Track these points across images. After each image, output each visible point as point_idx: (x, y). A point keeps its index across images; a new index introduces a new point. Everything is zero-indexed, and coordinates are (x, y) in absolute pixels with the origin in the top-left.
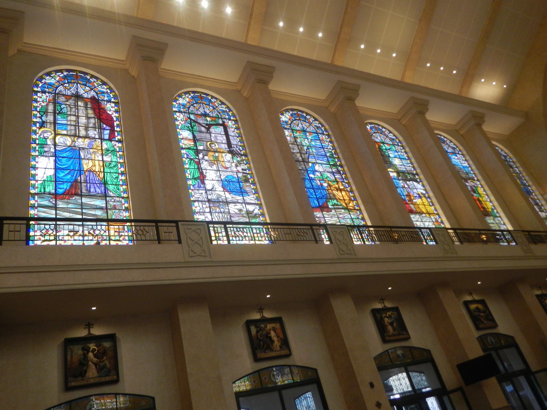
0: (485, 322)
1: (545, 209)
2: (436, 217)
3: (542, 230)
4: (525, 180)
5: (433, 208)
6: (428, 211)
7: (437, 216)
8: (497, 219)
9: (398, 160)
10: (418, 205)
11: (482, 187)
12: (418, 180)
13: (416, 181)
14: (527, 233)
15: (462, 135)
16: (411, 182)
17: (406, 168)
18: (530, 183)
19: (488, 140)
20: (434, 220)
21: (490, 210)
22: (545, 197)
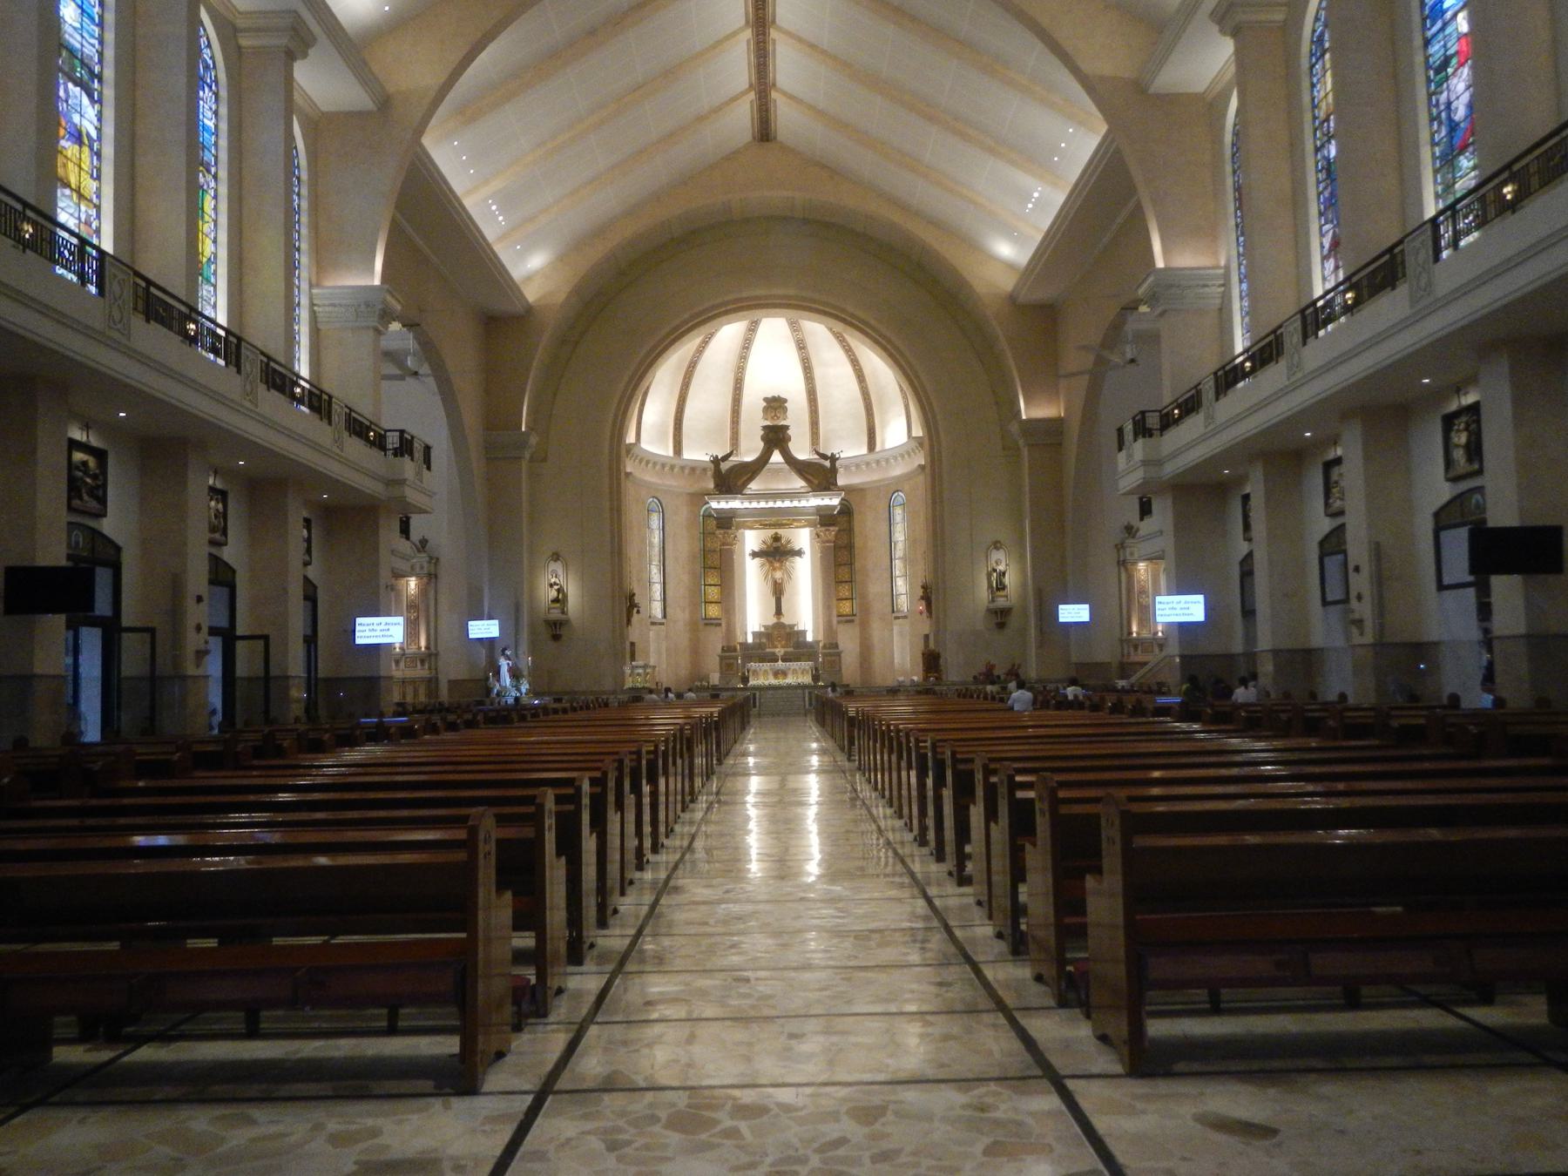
0: (86, 497)
1: (299, 316)
2: (90, 212)
3: (283, 361)
4: (299, 232)
5: (95, 184)
6: (79, 188)
7: (93, 212)
8: (206, 287)
9: (75, 10)
10: (66, 157)
11: (215, 197)
12: (96, 93)
13: (90, 95)
14: (265, 360)
15: (239, 47)
16: (78, 89)
17: (82, 45)
18: (304, 246)
19: (289, 108)
20: (83, 217)
21: (205, 260)
22: (315, 291)
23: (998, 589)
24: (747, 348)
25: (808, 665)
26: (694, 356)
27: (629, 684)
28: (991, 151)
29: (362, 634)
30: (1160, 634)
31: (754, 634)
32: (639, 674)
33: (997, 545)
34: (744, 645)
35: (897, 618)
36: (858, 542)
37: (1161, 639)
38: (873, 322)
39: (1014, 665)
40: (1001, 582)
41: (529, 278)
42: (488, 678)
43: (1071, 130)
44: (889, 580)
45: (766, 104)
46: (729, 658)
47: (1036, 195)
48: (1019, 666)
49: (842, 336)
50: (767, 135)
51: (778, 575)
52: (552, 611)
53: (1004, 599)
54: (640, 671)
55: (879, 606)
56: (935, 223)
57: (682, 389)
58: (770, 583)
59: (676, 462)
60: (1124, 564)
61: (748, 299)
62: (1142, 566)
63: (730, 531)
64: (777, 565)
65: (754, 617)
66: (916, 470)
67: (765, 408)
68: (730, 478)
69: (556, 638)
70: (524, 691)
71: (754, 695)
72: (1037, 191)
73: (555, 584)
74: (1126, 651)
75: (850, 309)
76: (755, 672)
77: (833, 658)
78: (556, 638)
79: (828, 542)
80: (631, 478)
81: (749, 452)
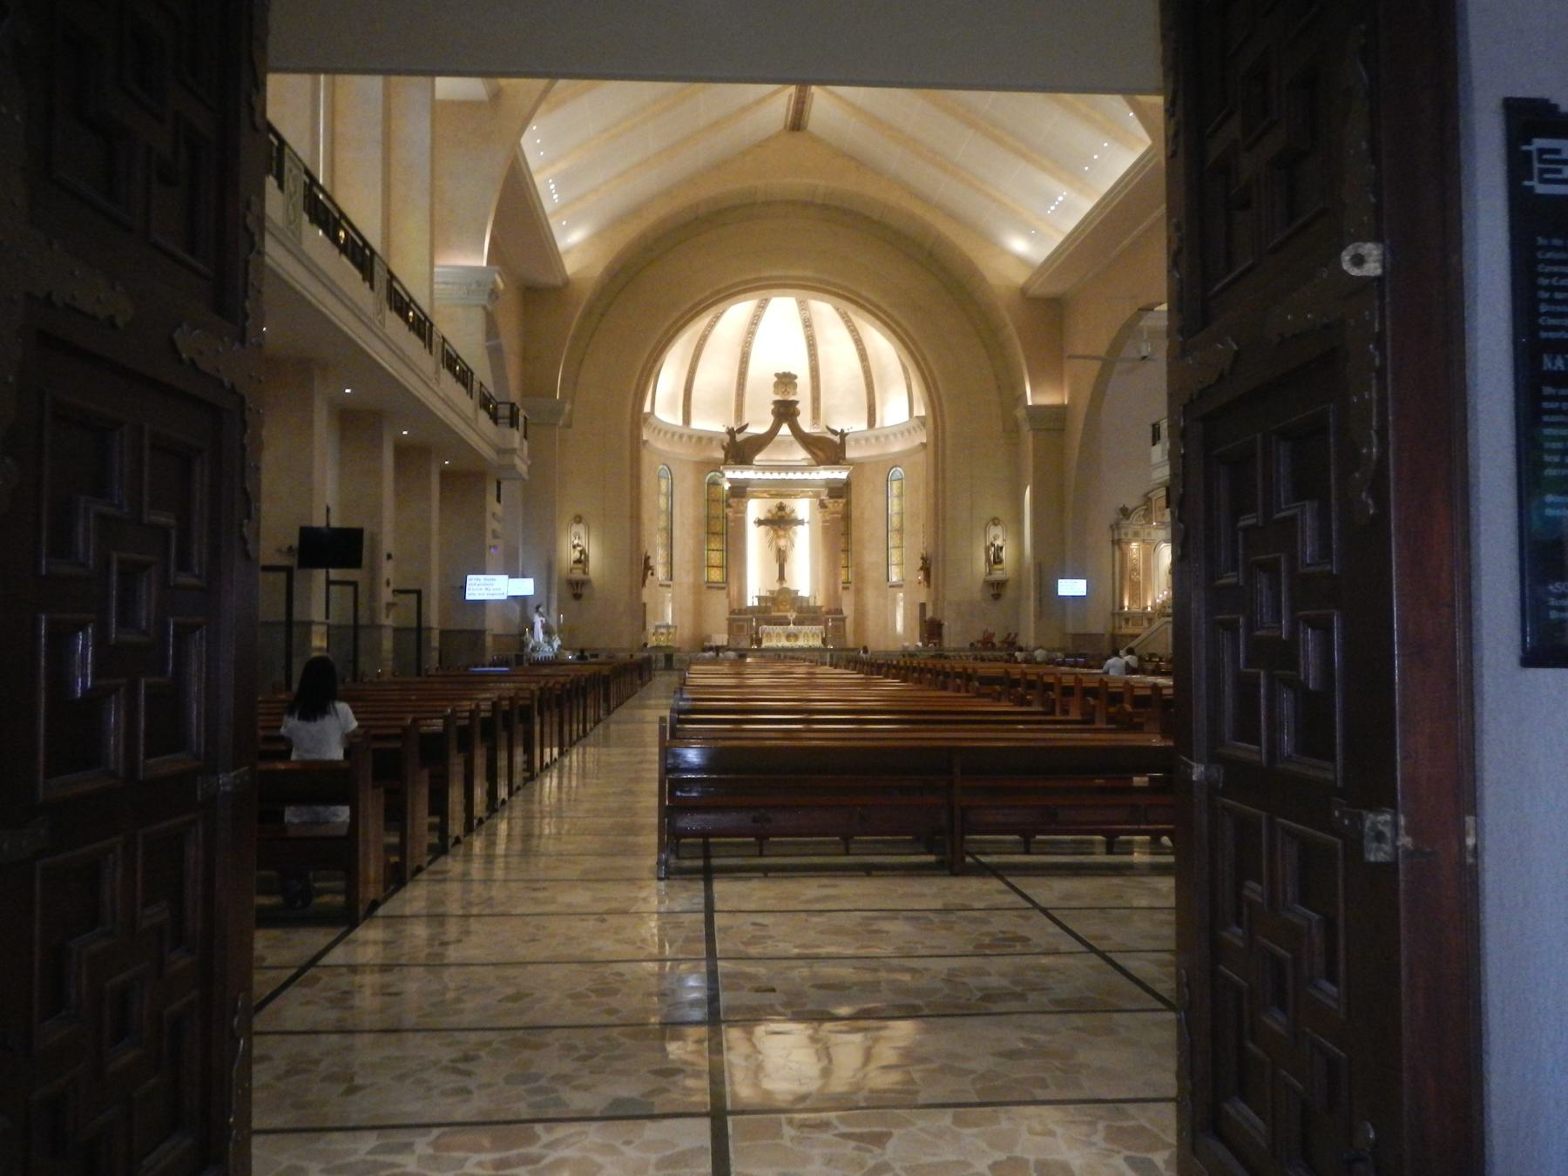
23: (995, 563)
24: (756, 324)
25: (818, 629)
26: (706, 330)
28: (1024, 156)
29: (472, 587)
30: (1149, 609)
31: (760, 598)
32: (662, 634)
33: (995, 521)
35: (891, 587)
36: (855, 513)
37: (1149, 613)
38: (885, 306)
39: (1009, 635)
40: (998, 557)
41: (568, 251)
42: (523, 634)
43: (1106, 145)
45: (804, 97)
46: (735, 620)
47: (1060, 199)
48: (1016, 635)
49: (846, 313)
50: (799, 125)
51: (782, 543)
53: (1000, 572)
54: (664, 630)
55: (873, 575)
56: (952, 216)
58: (774, 550)
59: (686, 431)
60: (1117, 543)
61: (767, 279)
62: (1134, 545)
63: (744, 500)
64: (781, 533)
65: (756, 583)
66: (918, 446)
67: (775, 383)
68: (741, 449)
69: (577, 597)
70: (556, 646)
72: (1062, 195)
73: (578, 545)
74: (1117, 621)
75: (864, 293)
76: (769, 635)
77: (838, 623)
78: (577, 597)
79: (837, 513)
81: (759, 425)
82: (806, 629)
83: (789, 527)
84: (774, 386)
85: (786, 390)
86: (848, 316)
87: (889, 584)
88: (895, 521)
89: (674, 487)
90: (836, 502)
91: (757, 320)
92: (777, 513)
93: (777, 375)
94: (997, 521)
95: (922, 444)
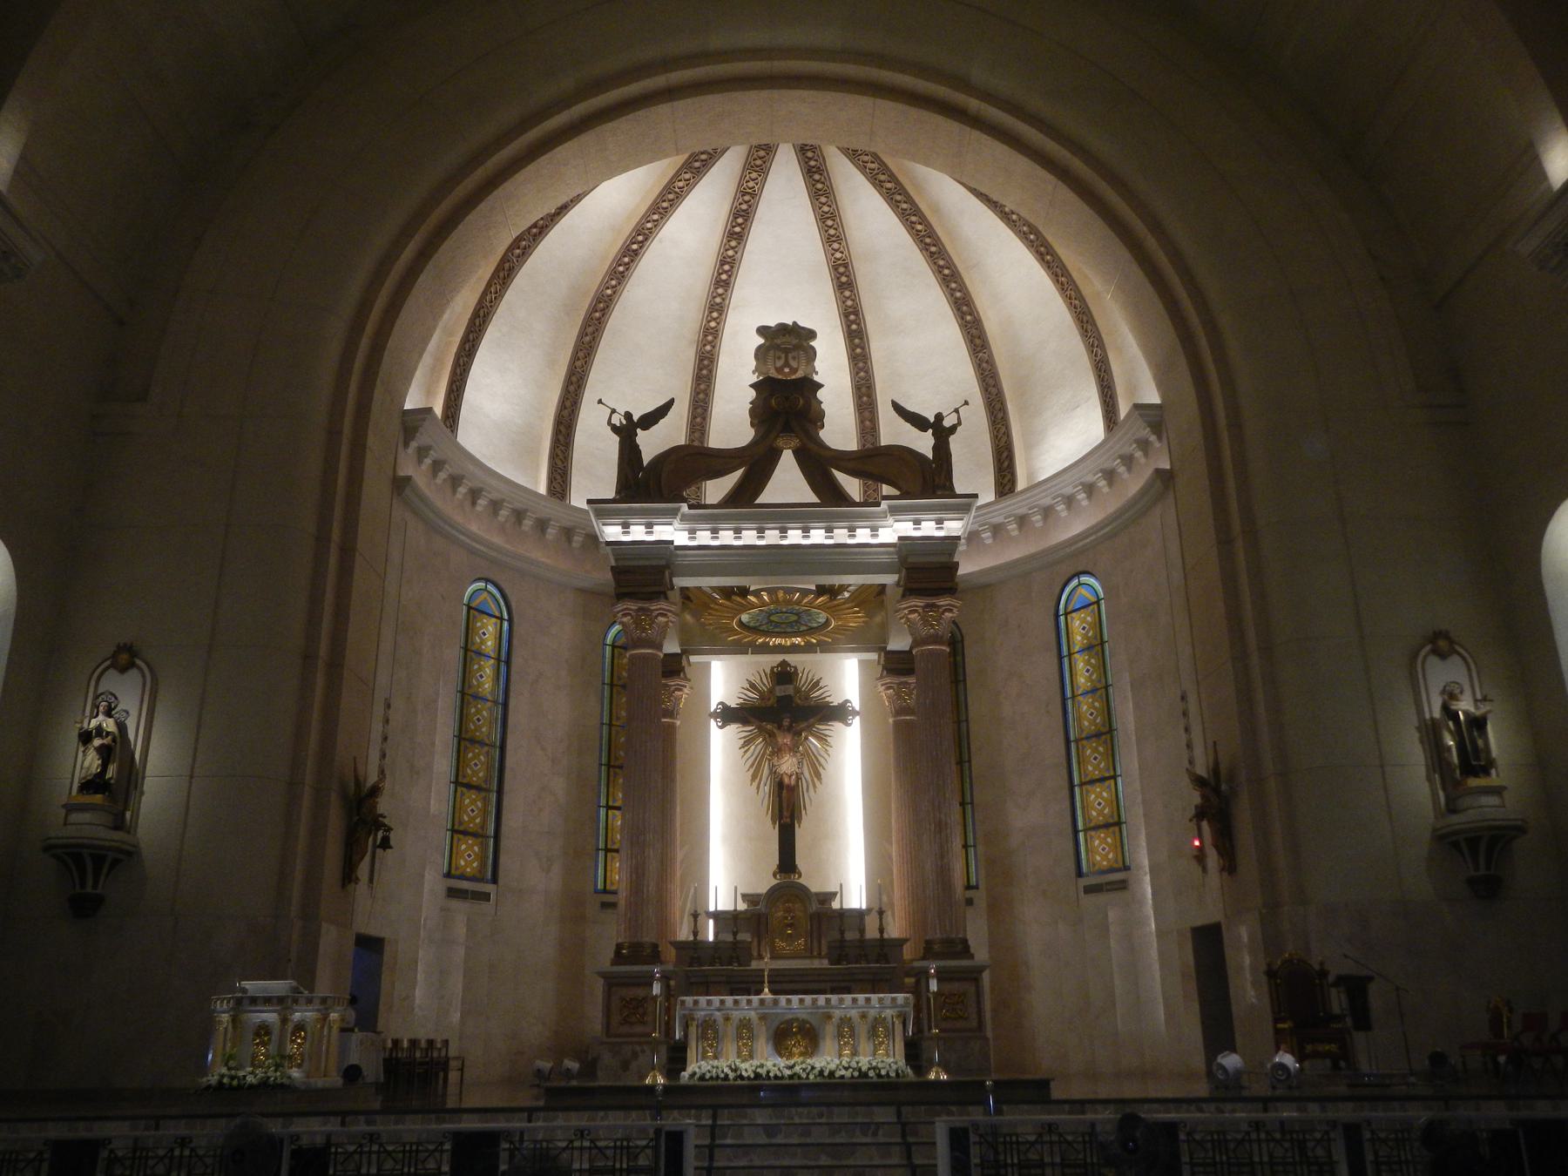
25: (888, 1004)
27: (217, 1072)
32: (263, 1030)
33: (1441, 644)
34: (693, 950)
35: (1089, 890)
44: (1065, 792)
51: (787, 765)
52: (74, 817)
53: (1492, 800)
54: (270, 1017)
57: (575, 358)
58: (766, 789)
59: (552, 509)
64: (785, 739)
69: (84, 906)
71: (675, 1140)
73: (100, 731)
76: (709, 1030)
77: (955, 987)
80: (408, 491)
82: (847, 1005)
83: (803, 725)
84: (756, 356)
85: (787, 364)
86: (937, 242)
87: (1083, 882)
88: (1086, 711)
89: (515, 642)
90: (932, 606)
91: (730, 273)
92: (771, 691)
93: (762, 331)
94: (1442, 644)
95: (1159, 472)
